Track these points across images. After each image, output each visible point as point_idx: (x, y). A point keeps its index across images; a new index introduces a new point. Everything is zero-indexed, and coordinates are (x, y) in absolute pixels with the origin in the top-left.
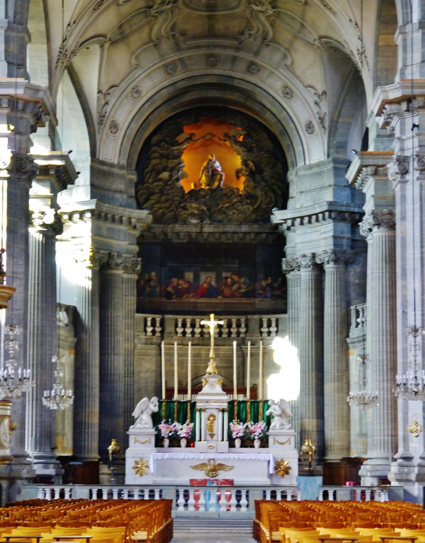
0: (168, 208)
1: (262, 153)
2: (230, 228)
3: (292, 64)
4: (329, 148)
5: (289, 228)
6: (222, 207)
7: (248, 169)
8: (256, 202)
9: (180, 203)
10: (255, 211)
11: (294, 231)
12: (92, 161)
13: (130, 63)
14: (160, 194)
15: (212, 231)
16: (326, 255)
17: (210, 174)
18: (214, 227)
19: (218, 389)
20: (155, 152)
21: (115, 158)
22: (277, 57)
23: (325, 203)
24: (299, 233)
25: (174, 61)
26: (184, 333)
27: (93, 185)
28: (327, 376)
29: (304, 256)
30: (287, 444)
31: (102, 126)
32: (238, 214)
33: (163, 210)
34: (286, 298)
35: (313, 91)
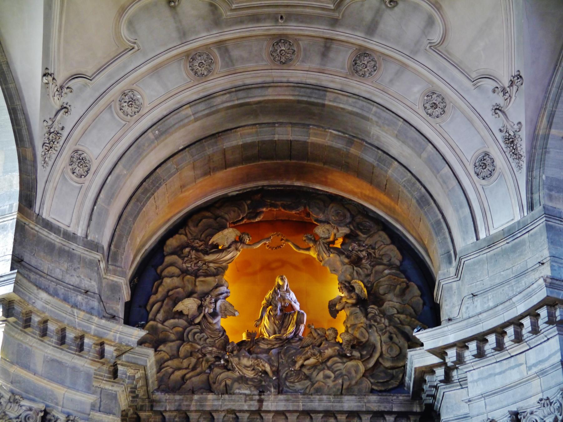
0: (194, 368)
1: (380, 268)
2: (320, 403)
3: (444, 38)
4: (530, 191)
5: (448, 379)
6: (302, 366)
7: (352, 294)
8: (371, 356)
9: (218, 358)
10: (369, 373)
11: (463, 384)
12: (20, 210)
13: (118, 35)
14: (178, 342)
15: (281, 408)
16: (547, 410)
17: (278, 312)
18: (287, 400)
20: (171, 264)
21: (78, 224)
22: (414, 27)
23: (541, 281)
24: (476, 378)
25: (207, 46)
31: (53, 154)
32: (336, 378)
33: (184, 372)
35: (489, 84)
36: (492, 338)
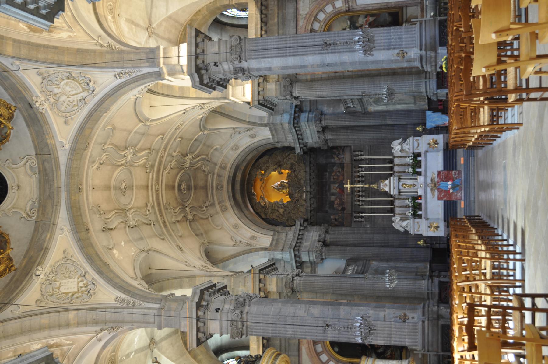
19: (387, 182)
26: (363, 201)
27: (282, 250)
28: (384, 123)
29: (319, 138)
30: (419, 141)
34: (344, 147)
36: (299, 136)
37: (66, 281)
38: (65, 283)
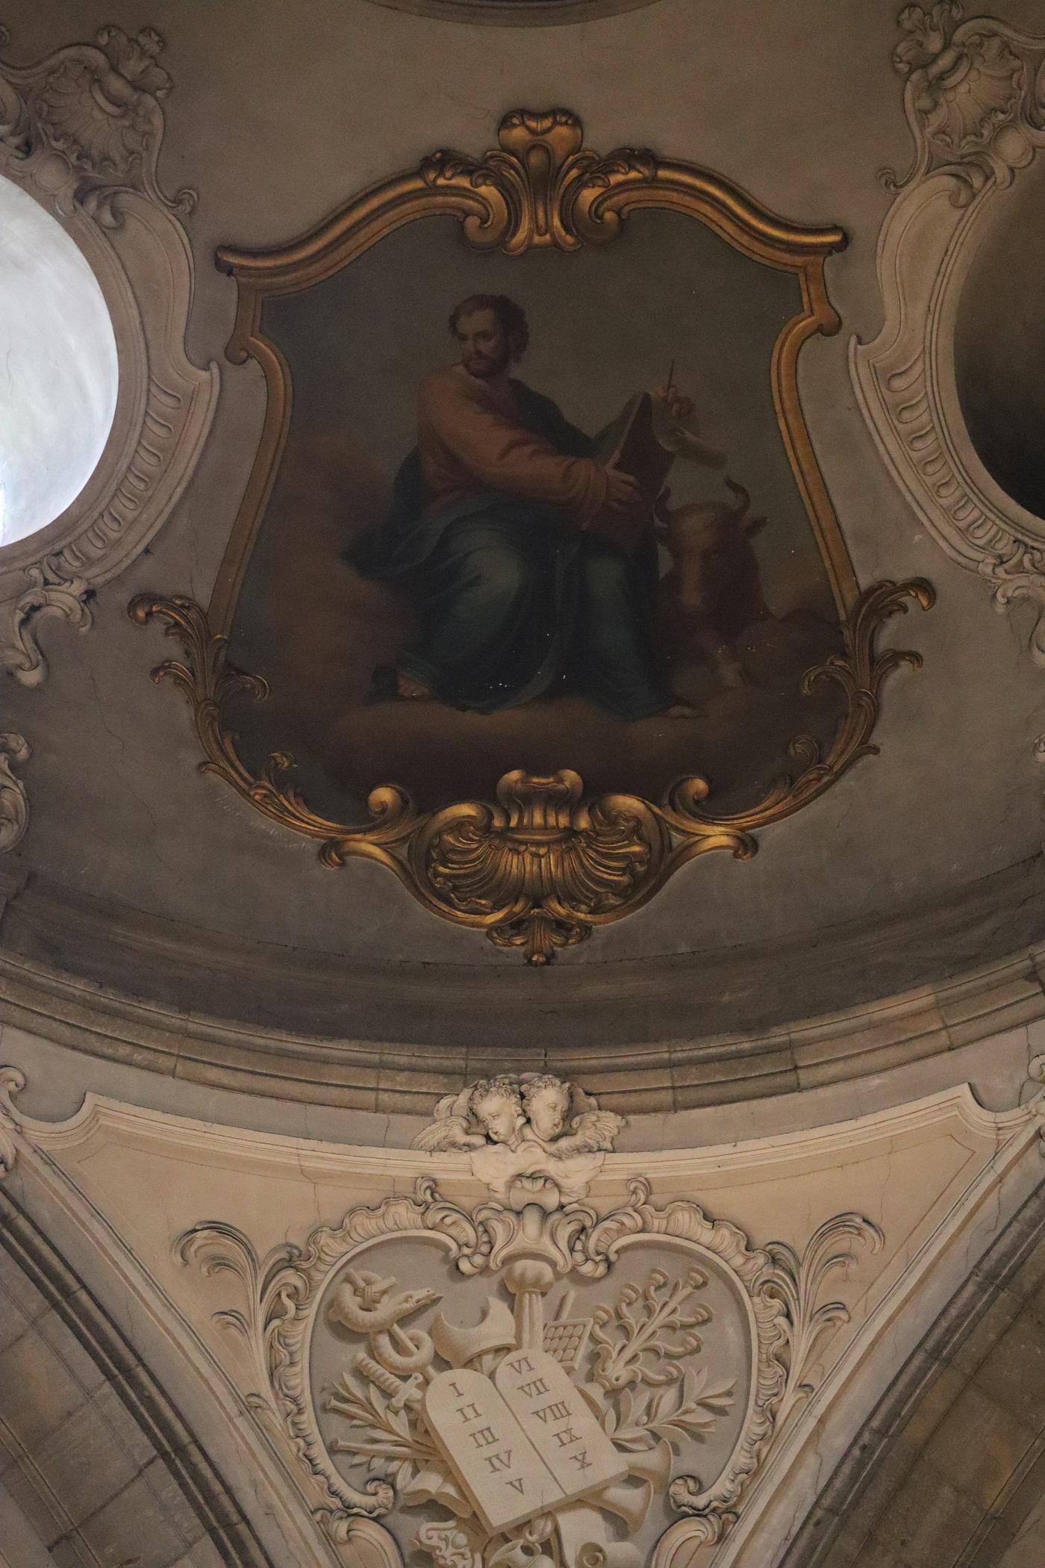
37: (561, 1386)
38: (540, 1386)
